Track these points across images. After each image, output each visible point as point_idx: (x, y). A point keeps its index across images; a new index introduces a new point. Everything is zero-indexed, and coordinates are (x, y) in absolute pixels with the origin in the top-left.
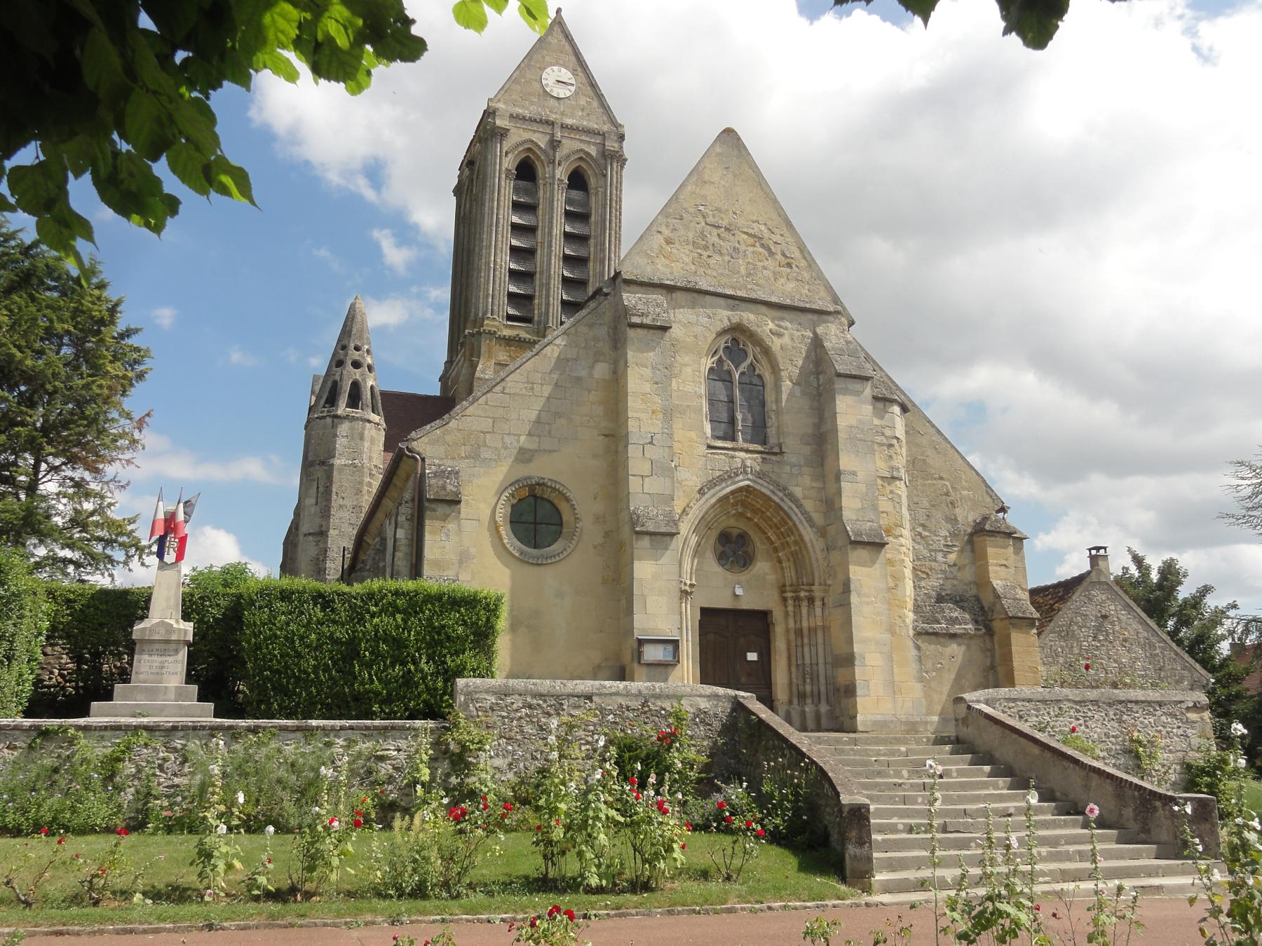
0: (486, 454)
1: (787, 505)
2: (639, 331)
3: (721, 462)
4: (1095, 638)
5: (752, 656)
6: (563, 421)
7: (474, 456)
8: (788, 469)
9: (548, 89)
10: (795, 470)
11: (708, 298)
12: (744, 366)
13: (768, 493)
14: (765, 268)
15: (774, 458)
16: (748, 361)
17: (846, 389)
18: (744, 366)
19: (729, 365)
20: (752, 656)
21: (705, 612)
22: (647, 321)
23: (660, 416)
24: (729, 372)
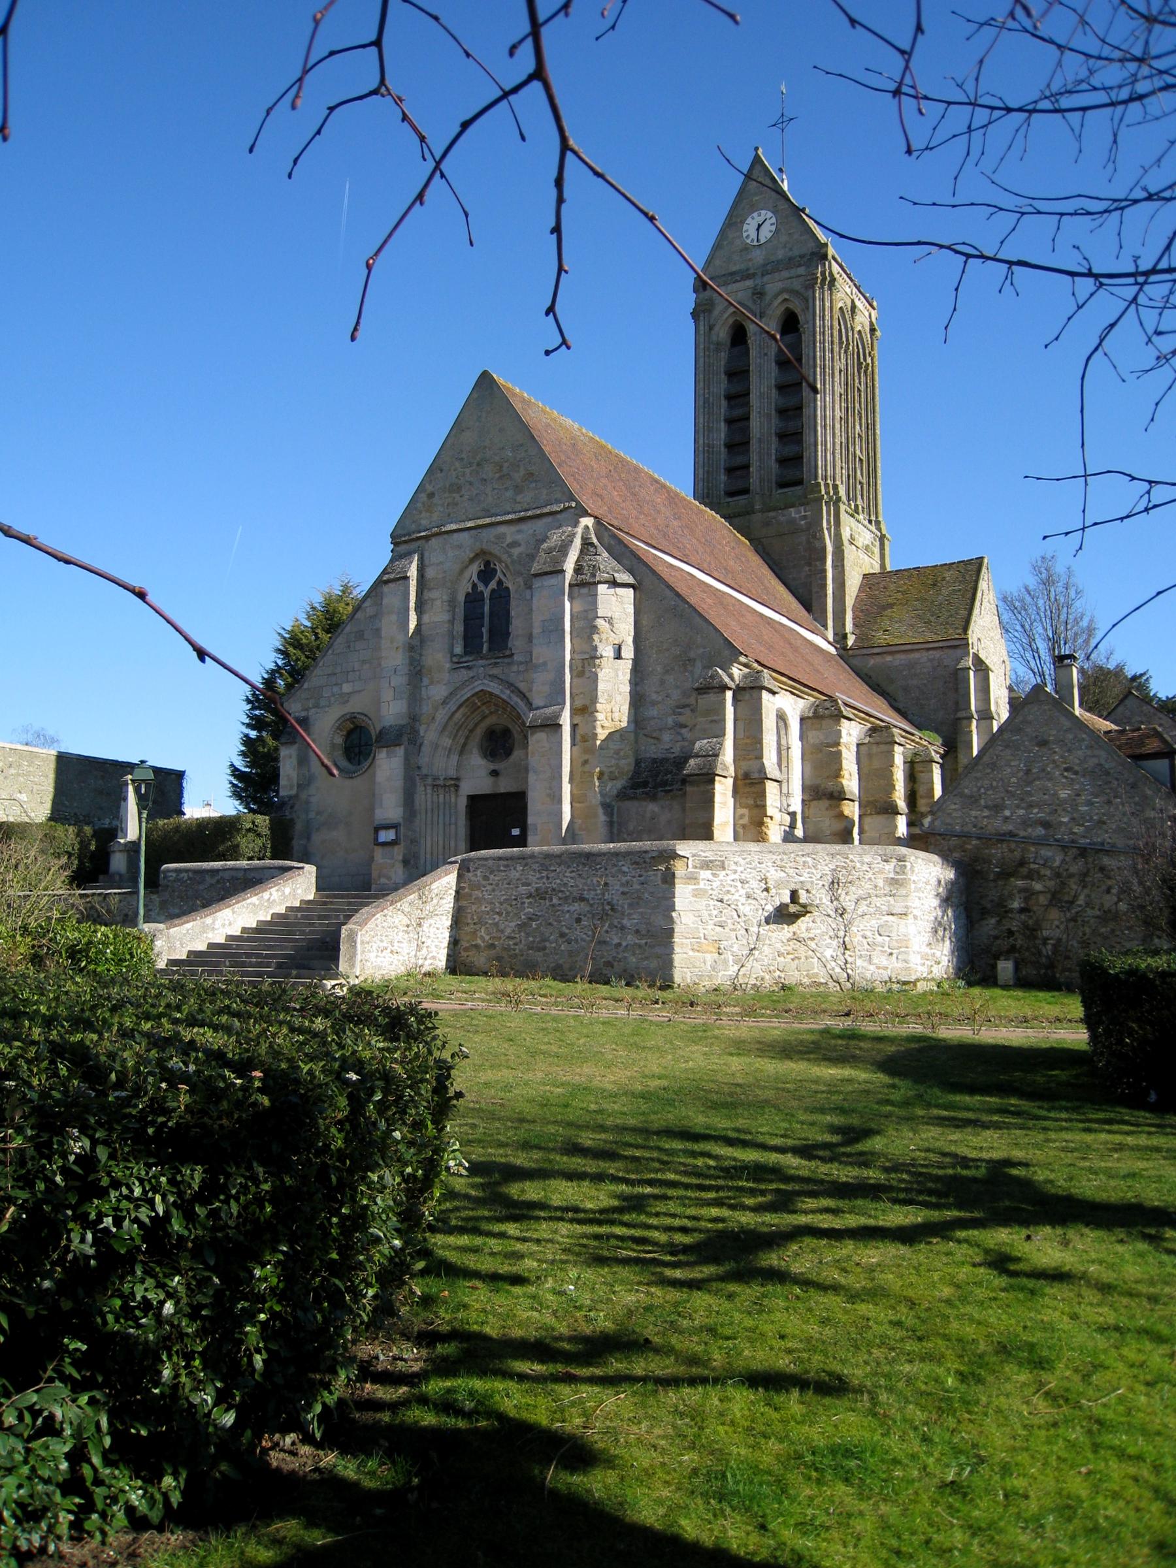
0: (323, 703)
1: (516, 700)
2: (390, 585)
3: (464, 674)
4: (1028, 772)
5: (516, 832)
6: (366, 666)
7: (317, 706)
8: (515, 668)
9: (748, 241)
10: (522, 668)
11: (455, 535)
12: (493, 585)
13: (497, 692)
14: (507, 489)
15: (506, 660)
16: (497, 578)
17: (542, 586)
18: (493, 585)
19: (481, 587)
20: (516, 832)
21: (472, 799)
22: (392, 576)
23: (401, 650)
24: (482, 592)
